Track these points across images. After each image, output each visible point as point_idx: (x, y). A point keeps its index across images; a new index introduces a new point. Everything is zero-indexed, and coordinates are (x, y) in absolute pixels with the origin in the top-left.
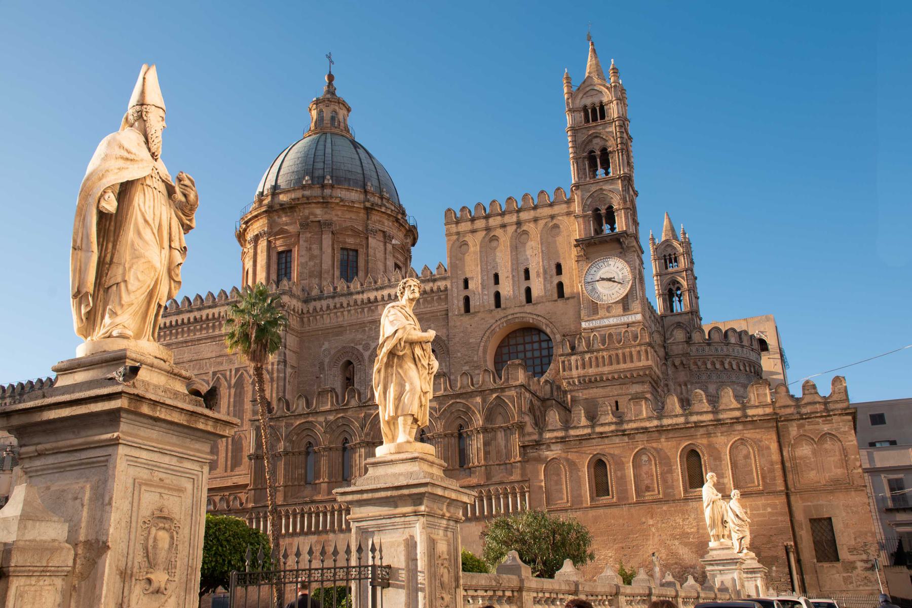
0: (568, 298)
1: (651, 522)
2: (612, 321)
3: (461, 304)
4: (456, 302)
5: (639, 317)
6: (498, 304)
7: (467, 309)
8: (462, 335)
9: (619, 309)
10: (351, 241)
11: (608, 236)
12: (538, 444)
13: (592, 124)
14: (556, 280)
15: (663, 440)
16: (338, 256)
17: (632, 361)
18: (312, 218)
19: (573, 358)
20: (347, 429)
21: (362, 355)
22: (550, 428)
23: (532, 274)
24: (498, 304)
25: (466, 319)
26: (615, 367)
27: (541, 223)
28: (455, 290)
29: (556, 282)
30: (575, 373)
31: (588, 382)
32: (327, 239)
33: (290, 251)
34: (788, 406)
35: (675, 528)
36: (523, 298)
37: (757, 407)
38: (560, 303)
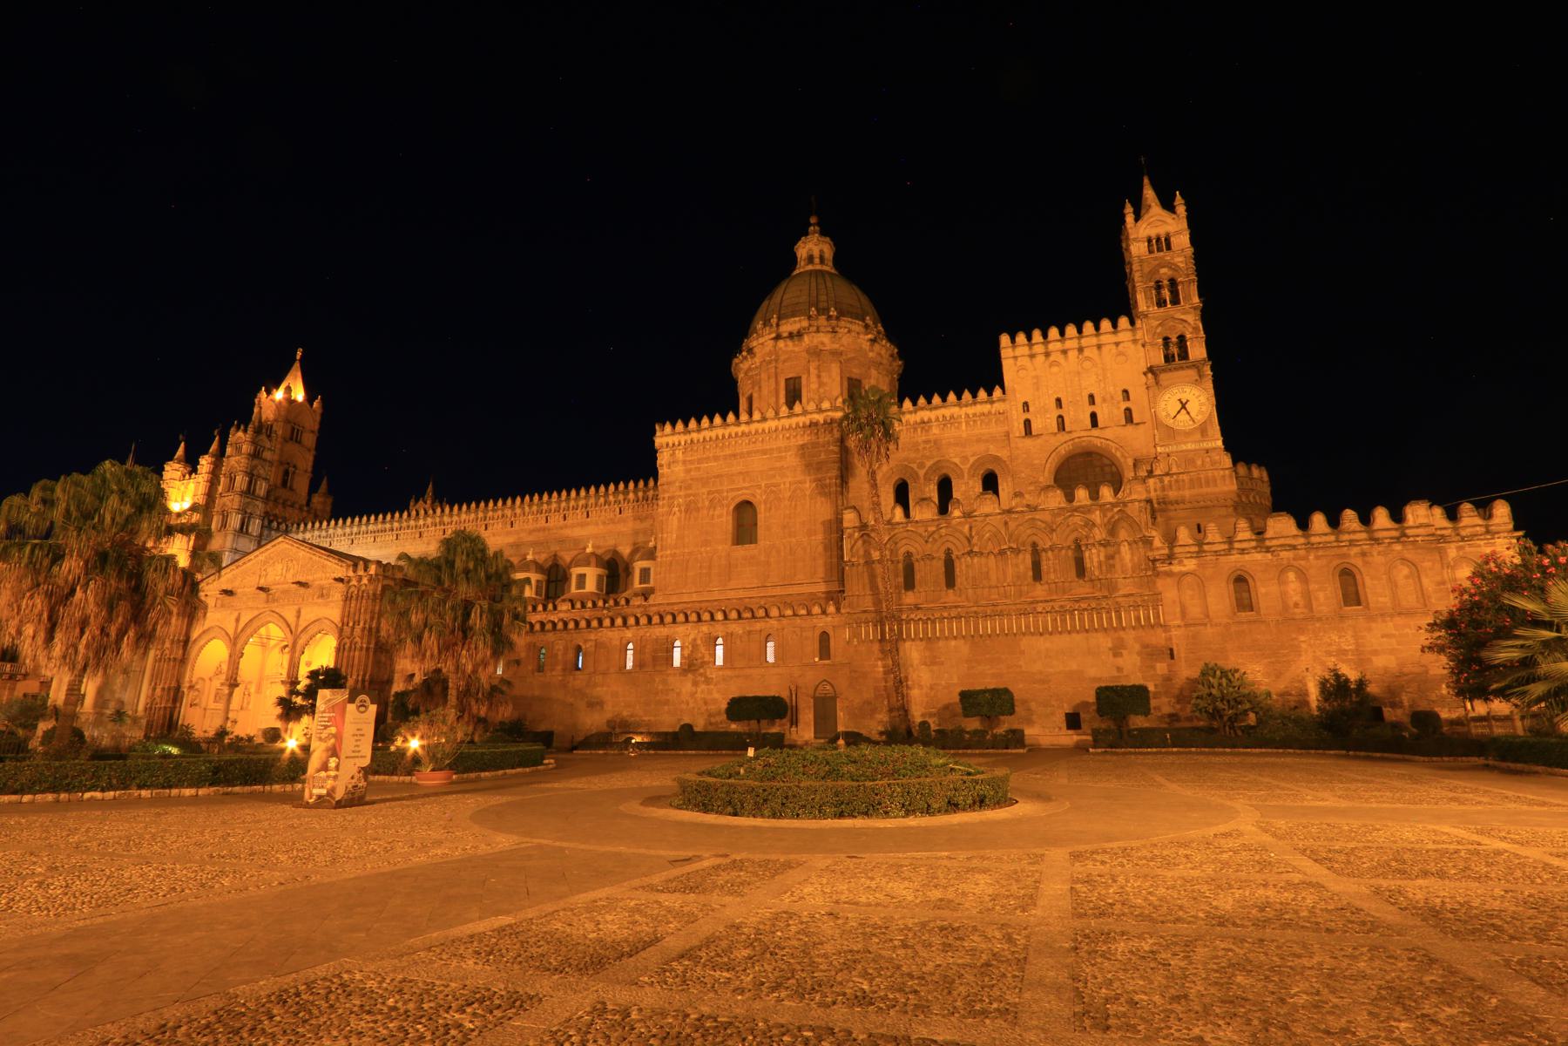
0: (1137, 424)
1: (1302, 638)
2: (1190, 446)
3: (1022, 426)
4: (1016, 424)
8: (1025, 456)
9: (1198, 436)
12: (1170, 558)
13: (1157, 254)
14: (1124, 405)
15: (1311, 557)
17: (1216, 486)
18: (821, 347)
20: (951, 539)
21: (917, 474)
22: (1181, 543)
23: (1097, 400)
25: (1028, 442)
26: (1196, 491)
27: (1105, 349)
28: (1014, 412)
29: (1123, 407)
32: (835, 369)
34: (1445, 528)
35: (1330, 645)
37: (1417, 527)
38: (1130, 428)
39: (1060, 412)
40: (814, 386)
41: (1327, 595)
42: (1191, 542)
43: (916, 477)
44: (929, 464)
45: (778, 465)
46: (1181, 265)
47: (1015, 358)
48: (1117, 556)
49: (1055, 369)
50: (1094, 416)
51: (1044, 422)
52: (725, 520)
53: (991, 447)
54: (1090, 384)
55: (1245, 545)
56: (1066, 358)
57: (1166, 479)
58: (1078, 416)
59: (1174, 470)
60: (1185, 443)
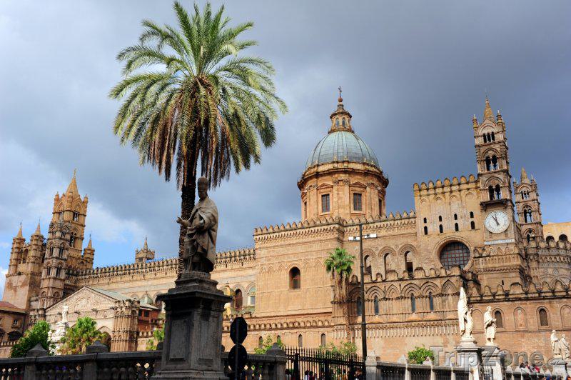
1: (523, 340)
2: (500, 242)
3: (423, 230)
5: (513, 241)
6: (441, 230)
7: (426, 232)
9: (503, 236)
10: (358, 190)
11: (497, 200)
16: (352, 197)
19: (481, 259)
23: (458, 217)
24: (441, 230)
25: (426, 237)
26: (501, 264)
30: (481, 266)
31: (488, 271)
32: (346, 188)
33: (329, 195)
36: (454, 229)
38: (473, 231)
39: (441, 223)
40: (335, 200)
41: (534, 320)
42: (478, 295)
43: (373, 255)
44: (380, 248)
45: (310, 250)
46: (498, 149)
47: (421, 196)
48: (447, 301)
49: (439, 201)
50: (456, 225)
51: (434, 228)
52: (286, 276)
53: (409, 240)
54: (455, 208)
55: (500, 297)
56: (444, 197)
57: (488, 258)
58: (449, 225)
59: (492, 254)
60: (497, 240)
